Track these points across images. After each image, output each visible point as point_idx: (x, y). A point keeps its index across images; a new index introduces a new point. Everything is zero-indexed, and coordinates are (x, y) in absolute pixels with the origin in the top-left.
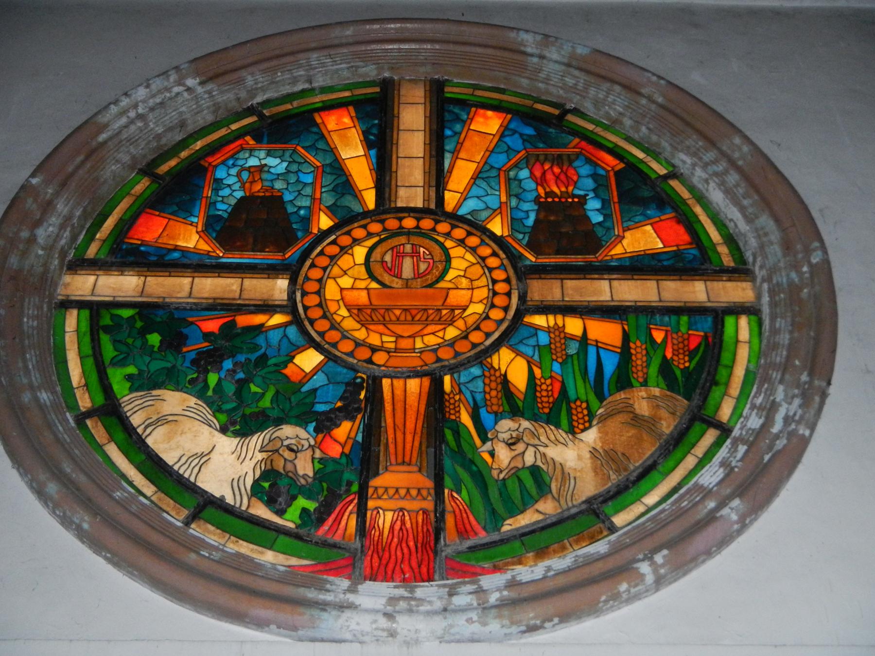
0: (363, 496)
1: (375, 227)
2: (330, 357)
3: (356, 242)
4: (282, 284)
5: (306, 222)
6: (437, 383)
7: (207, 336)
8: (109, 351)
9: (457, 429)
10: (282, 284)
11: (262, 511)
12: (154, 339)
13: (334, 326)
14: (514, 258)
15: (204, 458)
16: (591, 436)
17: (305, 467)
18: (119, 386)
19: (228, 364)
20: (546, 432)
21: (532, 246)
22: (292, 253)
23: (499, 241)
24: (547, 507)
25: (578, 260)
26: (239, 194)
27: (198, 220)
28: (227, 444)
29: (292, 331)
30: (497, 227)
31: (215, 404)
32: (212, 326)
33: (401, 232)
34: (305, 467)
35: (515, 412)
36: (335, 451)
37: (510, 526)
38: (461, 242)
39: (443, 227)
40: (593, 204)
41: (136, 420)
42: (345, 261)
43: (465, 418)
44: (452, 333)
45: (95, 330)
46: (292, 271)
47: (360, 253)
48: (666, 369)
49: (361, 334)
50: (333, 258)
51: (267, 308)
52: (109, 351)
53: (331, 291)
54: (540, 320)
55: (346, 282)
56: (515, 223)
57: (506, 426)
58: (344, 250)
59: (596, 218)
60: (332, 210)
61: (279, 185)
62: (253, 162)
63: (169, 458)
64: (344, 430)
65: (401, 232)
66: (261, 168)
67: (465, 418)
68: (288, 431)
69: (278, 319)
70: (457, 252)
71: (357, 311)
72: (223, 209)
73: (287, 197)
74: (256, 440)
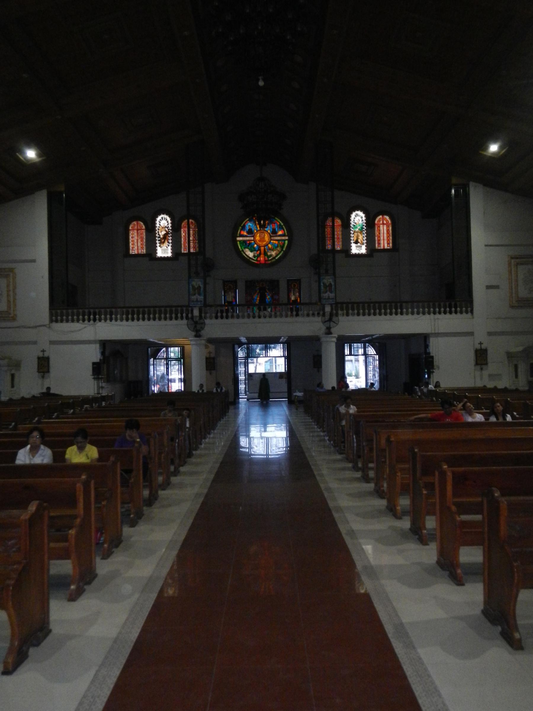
0: (260, 257)
1: (259, 232)
2: (257, 245)
3: (258, 233)
4: (253, 238)
5: (254, 231)
6: (265, 247)
7: (248, 243)
8: (241, 245)
9: (266, 251)
10: (253, 238)
11: (254, 258)
12: (244, 244)
13: (257, 242)
14: (270, 235)
15: (249, 254)
16: (275, 252)
17: (256, 255)
18: (243, 249)
19: (250, 246)
20: (272, 252)
21: (272, 234)
22: (253, 235)
23: (269, 233)
24: (272, 258)
25: (275, 235)
26: (248, 228)
27: (245, 231)
28: (251, 253)
29: (254, 243)
30: (269, 232)
31: (249, 249)
32: (248, 242)
33: (261, 232)
34: (256, 255)
35: (270, 250)
36: (258, 253)
37: (269, 259)
38: (266, 233)
39: (265, 232)
40: (277, 229)
41: (245, 251)
42: (257, 235)
43: (267, 251)
44: (265, 243)
45: (240, 243)
46: (253, 236)
47: (258, 235)
48: (281, 246)
49: (259, 243)
50: (256, 235)
51: (252, 240)
52: (241, 245)
53: (257, 239)
54: (272, 241)
55: (258, 238)
56: (270, 231)
57: (269, 251)
58: (257, 234)
59: (277, 230)
60: (256, 230)
61: (251, 227)
62: (249, 224)
63: (247, 254)
64: (259, 252)
65: (261, 232)
66: (250, 225)
67: (267, 251)
68: (255, 252)
69: (253, 242)
70: (266, 234)
71: (258, 241)
72: (247, 230)
73: (252, 228)
74: (253, 253)
